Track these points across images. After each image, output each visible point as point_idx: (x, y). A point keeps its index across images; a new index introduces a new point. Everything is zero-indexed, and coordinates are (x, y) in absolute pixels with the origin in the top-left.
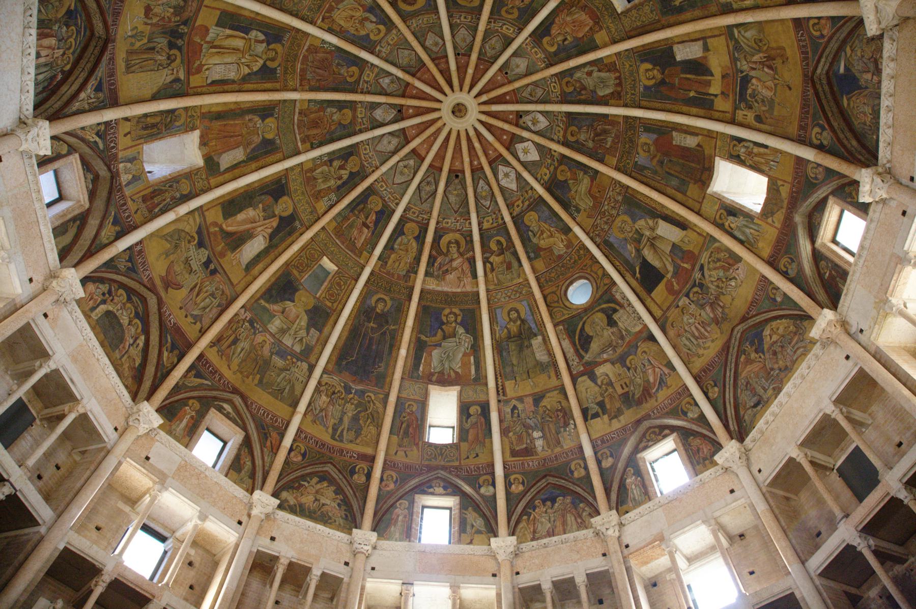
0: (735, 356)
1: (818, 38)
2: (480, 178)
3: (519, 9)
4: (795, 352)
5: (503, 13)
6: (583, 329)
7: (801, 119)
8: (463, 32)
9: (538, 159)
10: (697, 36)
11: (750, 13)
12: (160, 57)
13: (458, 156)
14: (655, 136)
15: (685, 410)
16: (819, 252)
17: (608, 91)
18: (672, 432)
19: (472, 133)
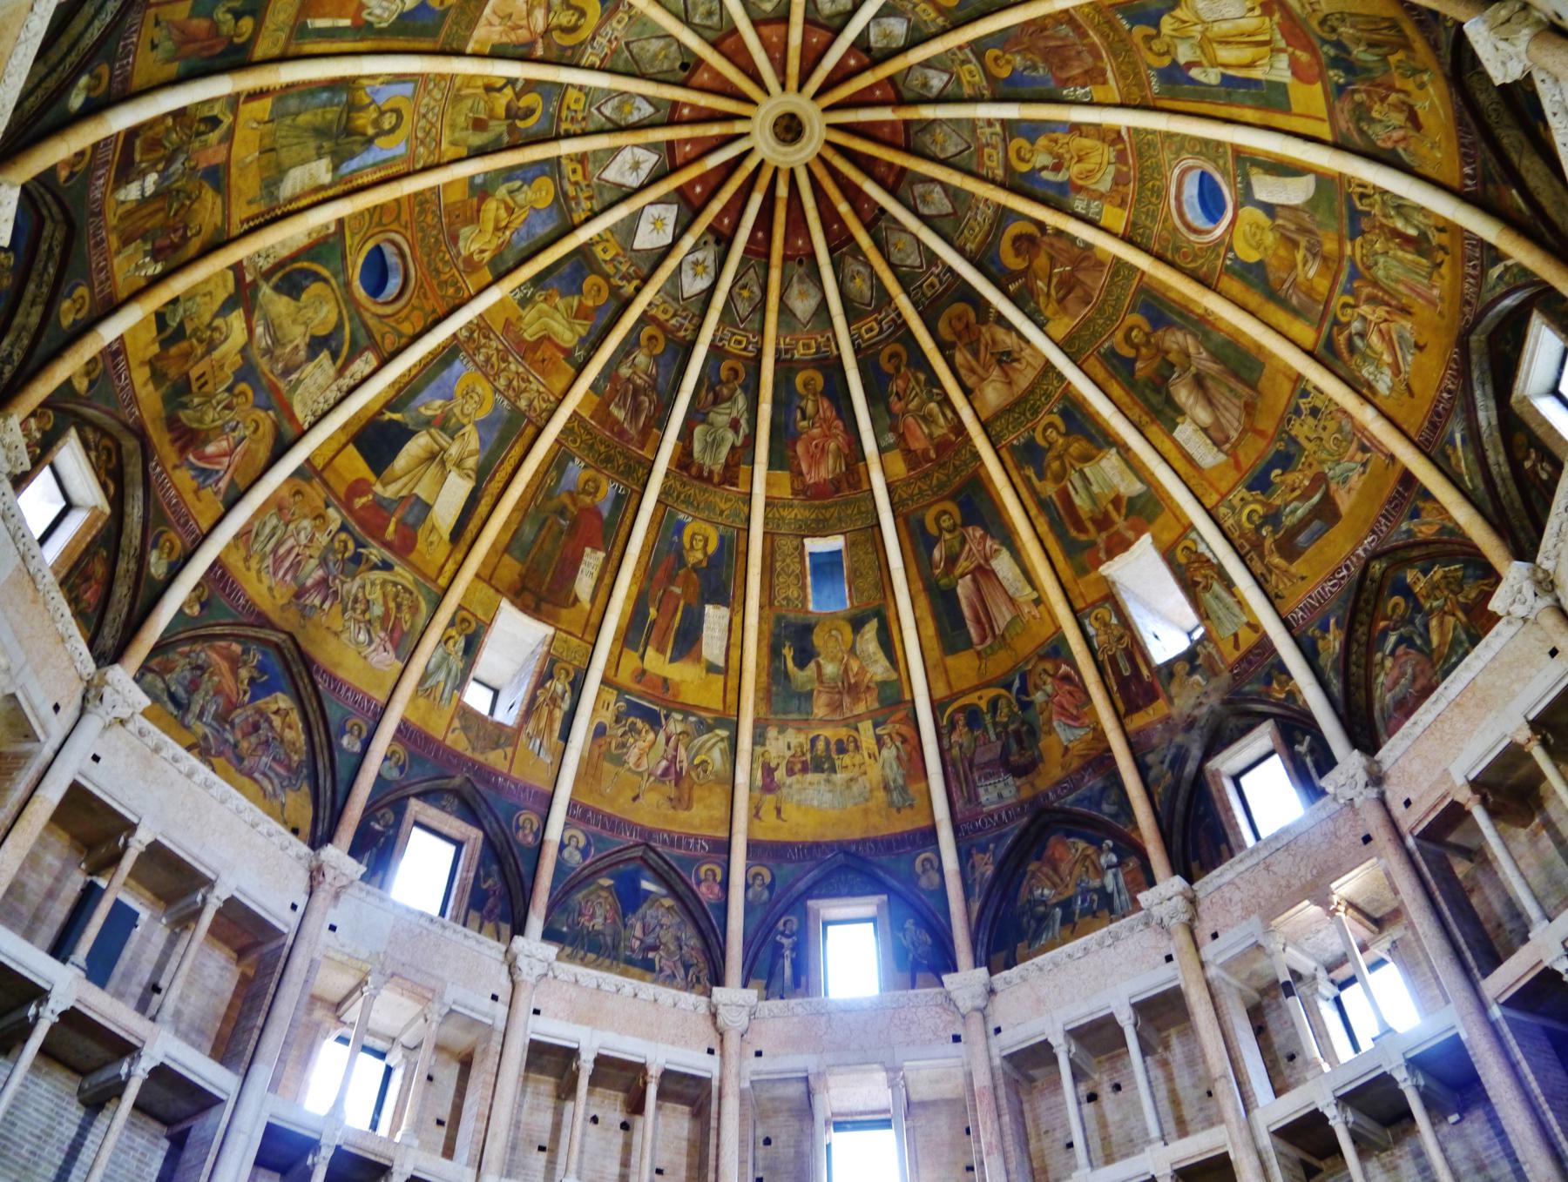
2: (657, 110)
3: (890, 377)
4: (264, 774)
5: (898, 348)
6: (317, 277)
7: (596, 812)
8: (914, 260)
9: (638, 245)
10: (734, 663)
13: (716, 85)
14: (605, 514)
15: (162, 541)
16: (404, 808)
17: (697, 447)
18: (111, 502)
19: (739, 127)
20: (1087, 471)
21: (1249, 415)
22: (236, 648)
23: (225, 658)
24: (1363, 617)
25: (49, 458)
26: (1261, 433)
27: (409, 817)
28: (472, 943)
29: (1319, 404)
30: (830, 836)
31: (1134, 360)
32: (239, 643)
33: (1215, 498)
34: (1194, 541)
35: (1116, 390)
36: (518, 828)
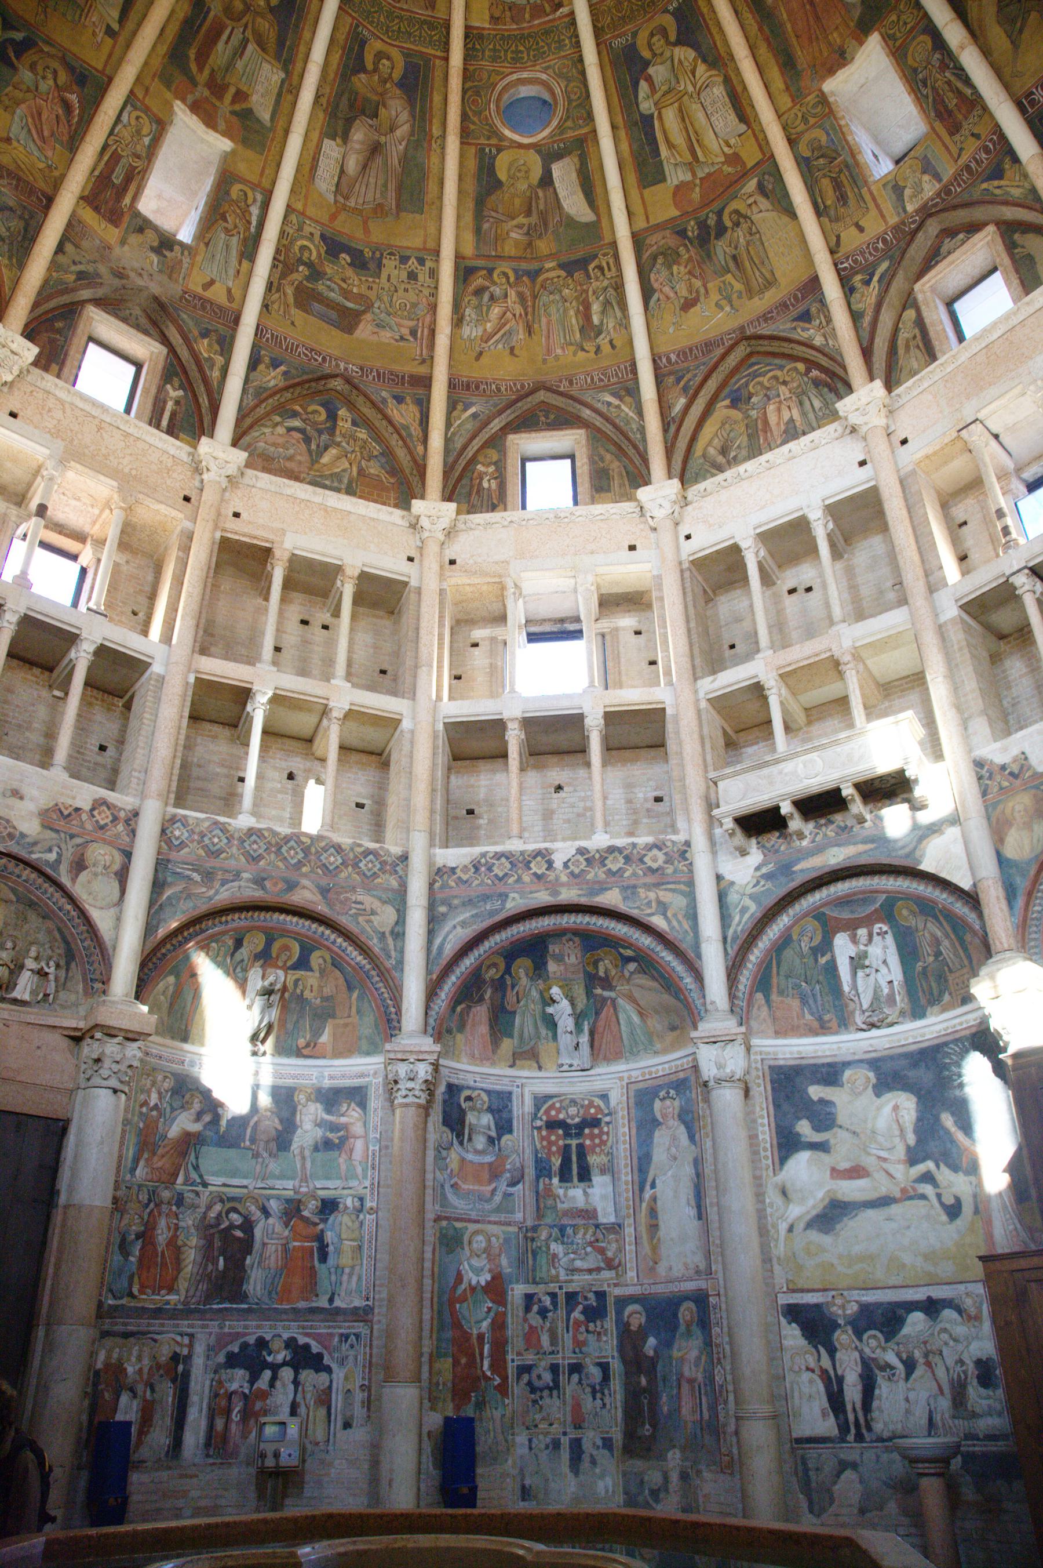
12: (741, 240)
20: (251, 47)
21: (375, 210)
24: (298, 390)
26: (367, 231)
29: (421, 277)
31: (363, 69)
33: (299, 206)
34: (255, 201)
35: (336, 57)
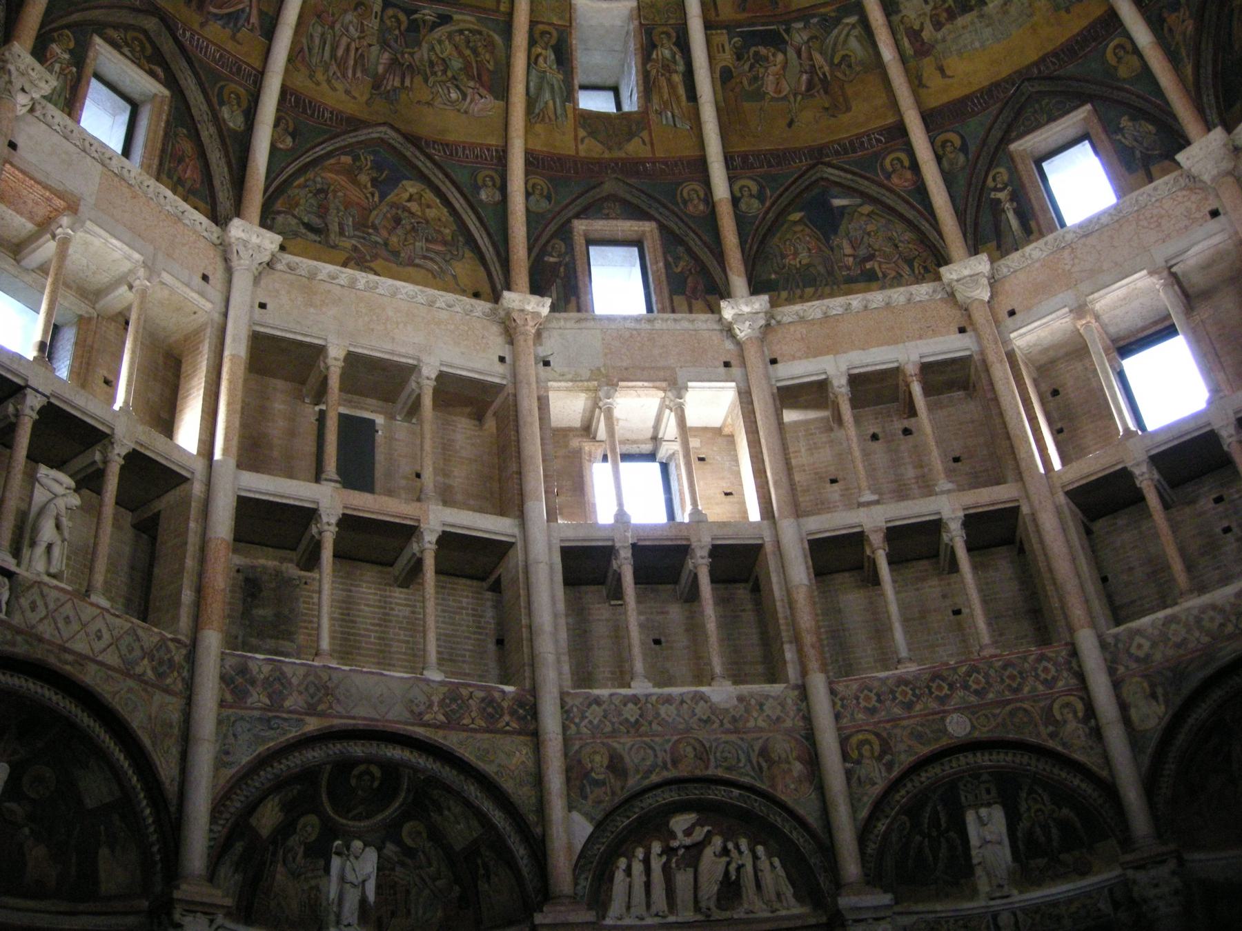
0: (343, 144)
1: (881, 165)
4: (425, 257)
7: (757, 155)
11: (897, 57)
16: (571, 232)
22: (346, 159)
23: (337, 173)
25: (89, 70)
27: (579, 241)
28: (686, 325)
30: (1005, 71)
32: (346, 154)
36: (685, 202)
